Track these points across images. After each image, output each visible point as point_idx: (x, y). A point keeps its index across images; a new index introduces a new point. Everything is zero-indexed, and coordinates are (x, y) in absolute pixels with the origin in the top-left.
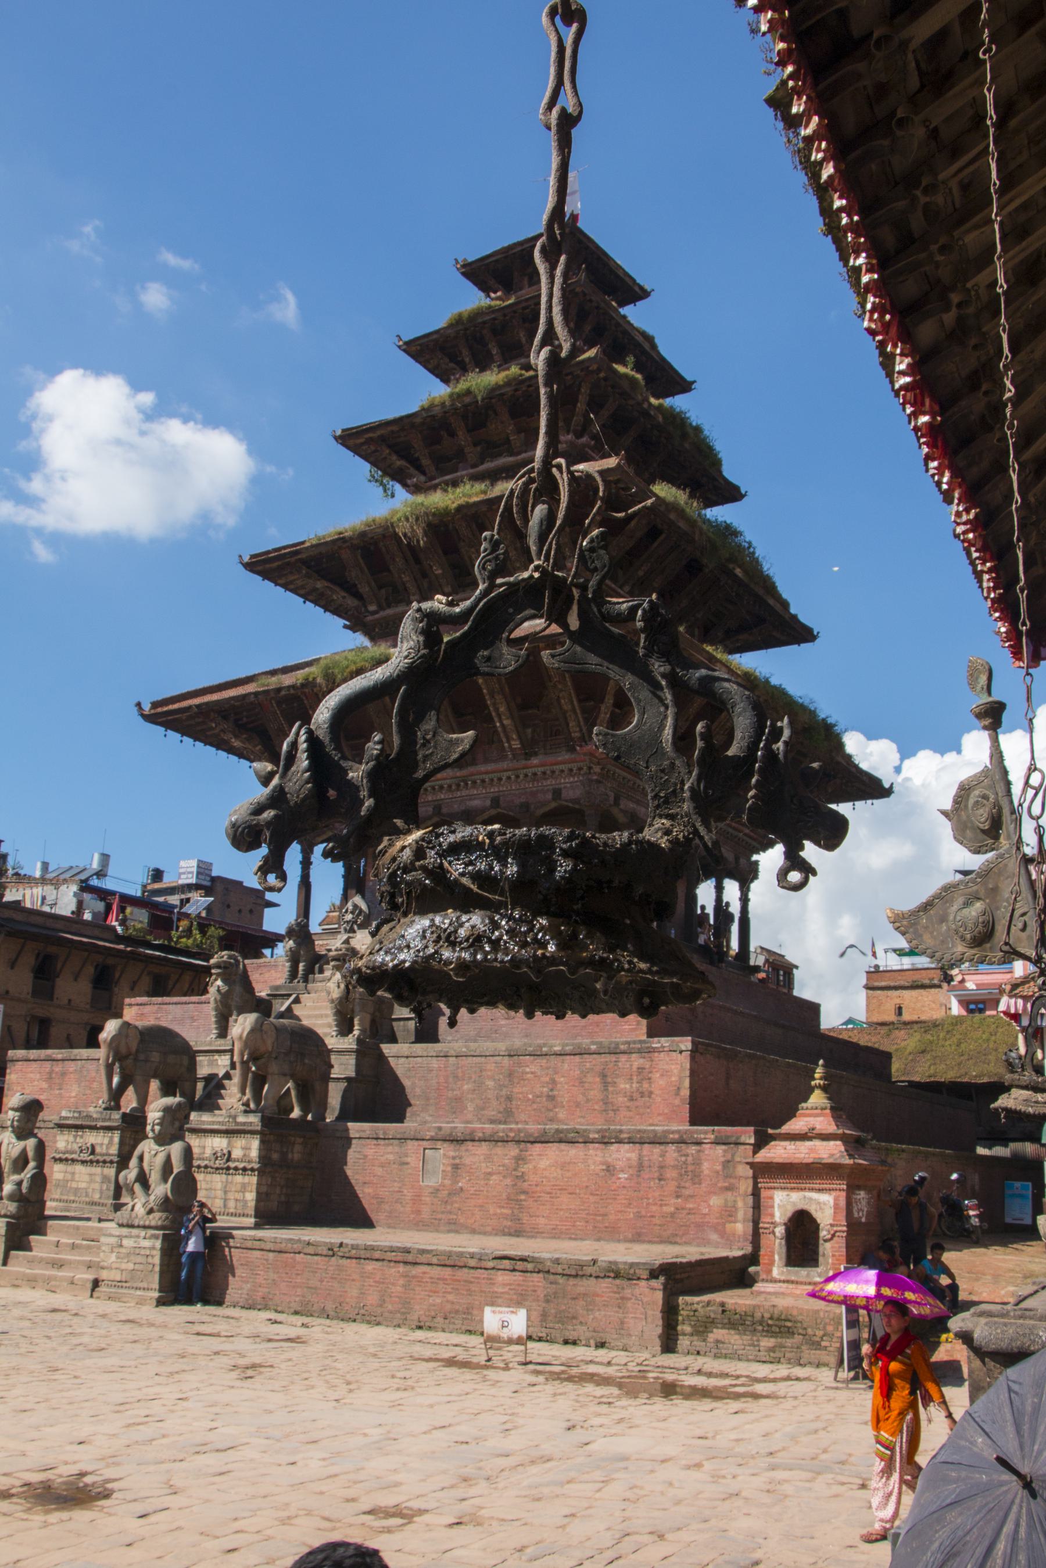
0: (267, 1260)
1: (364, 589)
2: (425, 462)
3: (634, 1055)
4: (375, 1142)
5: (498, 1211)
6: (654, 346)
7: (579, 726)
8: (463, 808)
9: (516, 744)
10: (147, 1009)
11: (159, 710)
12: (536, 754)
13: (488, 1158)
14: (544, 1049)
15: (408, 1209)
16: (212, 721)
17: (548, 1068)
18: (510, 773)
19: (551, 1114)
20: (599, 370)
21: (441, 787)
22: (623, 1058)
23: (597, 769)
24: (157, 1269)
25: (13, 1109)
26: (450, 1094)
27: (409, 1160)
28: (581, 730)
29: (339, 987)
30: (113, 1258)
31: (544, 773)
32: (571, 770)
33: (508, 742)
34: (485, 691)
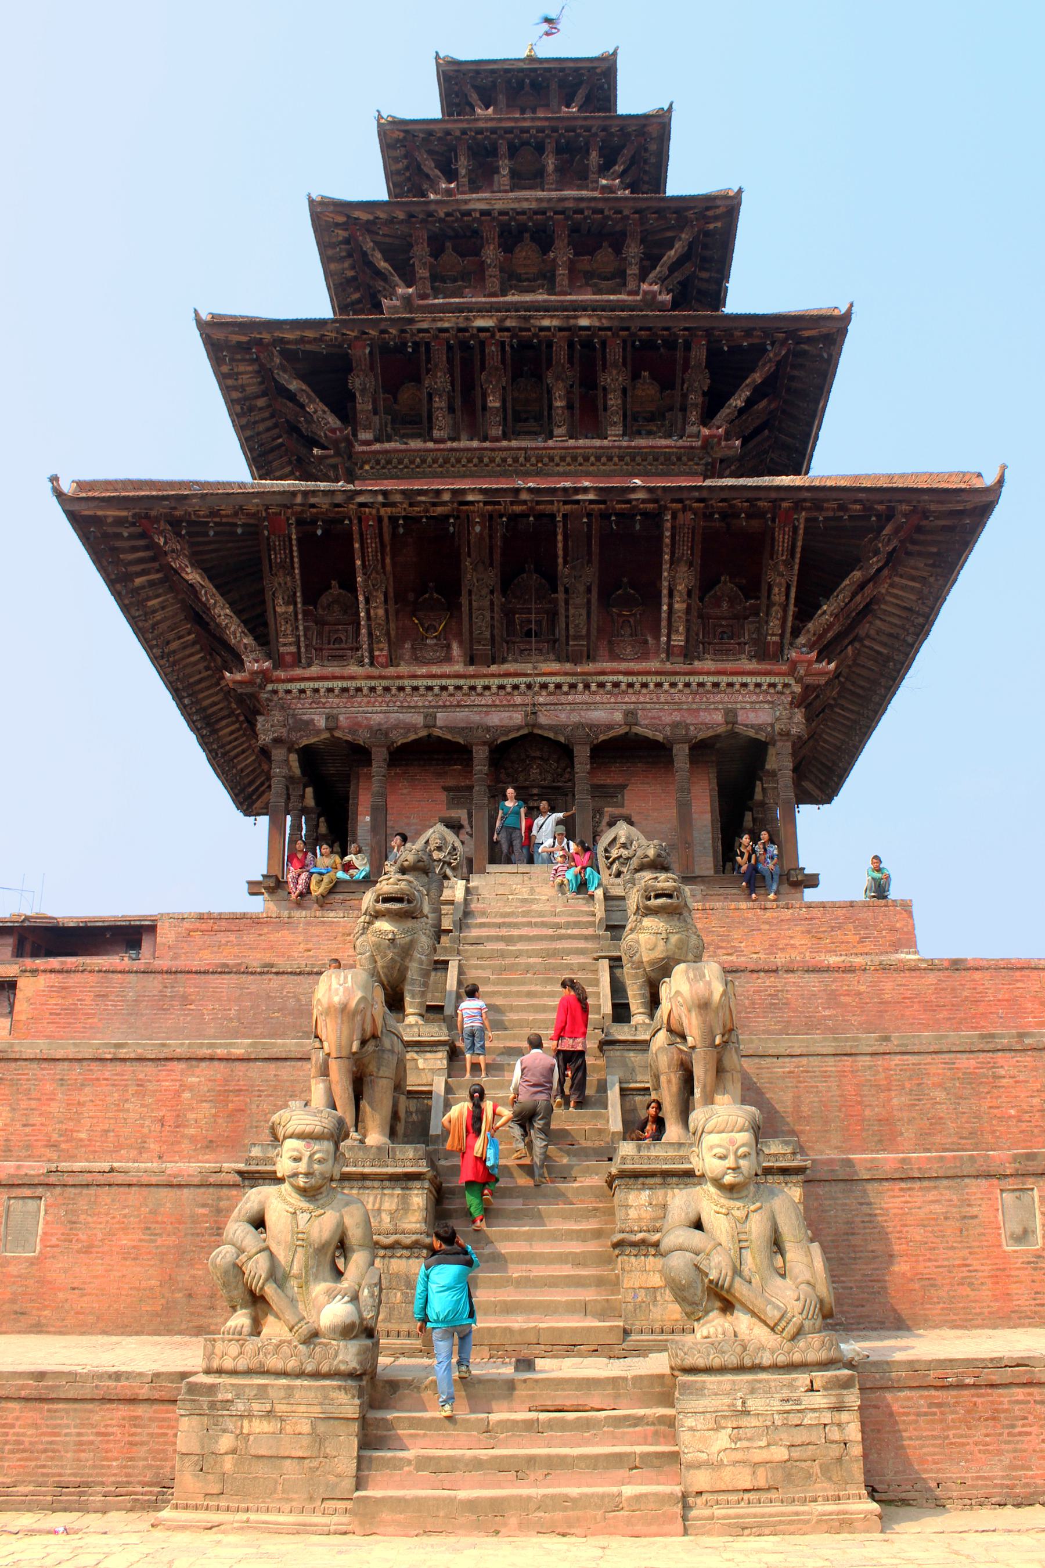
1: (363, 405)
2: (423, 272)
4: (903, 1185)
7: (783, 626)
8: (575, 718)
9: (679, 640)
10: (74, 980)
15: (986, 1293)
16: (161, 533)
18: (663, 678)
20: (716, 218)
21: (544, 686)
24: (857, 1450)
25: (300, 1136)
27: (975, 1211)
28: (782, 636)
29: (667, 940)
30: (722, 1440)
31: (716, 685)
32: (758, 685)
33: (669, 636)
34: (667, 557)
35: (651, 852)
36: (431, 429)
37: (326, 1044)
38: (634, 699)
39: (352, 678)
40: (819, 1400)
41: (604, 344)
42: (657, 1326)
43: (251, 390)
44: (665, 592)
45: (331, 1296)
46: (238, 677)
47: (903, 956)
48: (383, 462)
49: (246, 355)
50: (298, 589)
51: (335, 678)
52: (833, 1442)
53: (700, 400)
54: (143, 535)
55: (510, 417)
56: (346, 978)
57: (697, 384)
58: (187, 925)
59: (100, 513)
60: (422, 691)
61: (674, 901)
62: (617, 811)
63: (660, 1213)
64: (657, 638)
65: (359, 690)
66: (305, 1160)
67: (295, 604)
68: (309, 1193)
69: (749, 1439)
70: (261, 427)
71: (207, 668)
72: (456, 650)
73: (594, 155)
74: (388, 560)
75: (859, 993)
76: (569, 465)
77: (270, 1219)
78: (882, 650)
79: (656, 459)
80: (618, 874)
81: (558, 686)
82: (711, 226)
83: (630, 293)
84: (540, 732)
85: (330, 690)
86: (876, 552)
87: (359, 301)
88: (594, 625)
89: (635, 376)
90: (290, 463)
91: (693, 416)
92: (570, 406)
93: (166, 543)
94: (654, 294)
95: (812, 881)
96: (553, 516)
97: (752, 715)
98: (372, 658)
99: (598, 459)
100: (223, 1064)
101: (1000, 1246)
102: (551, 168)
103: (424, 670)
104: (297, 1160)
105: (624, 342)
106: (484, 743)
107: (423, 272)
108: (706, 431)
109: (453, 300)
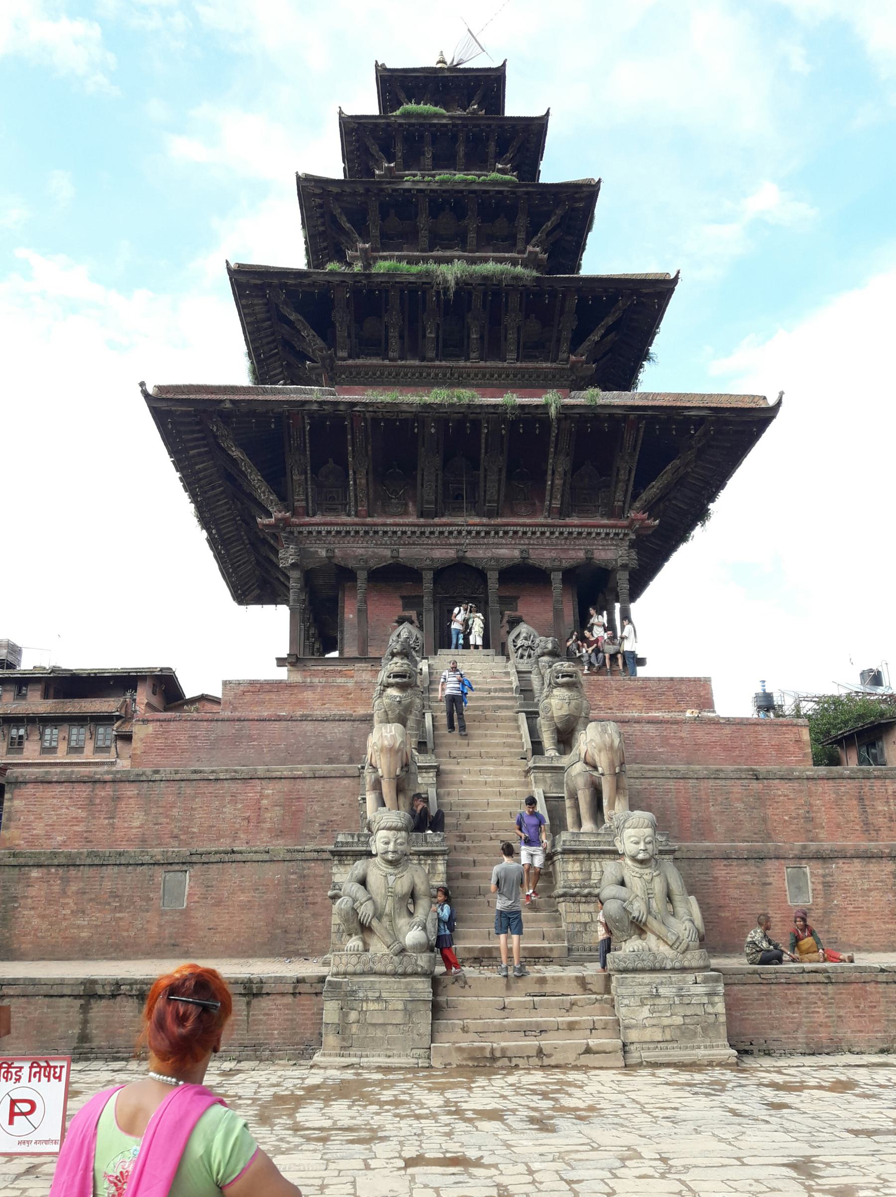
0: (826, 994)
1: (341, 333)
3: (887, 781)
4: (725, 862)
5: (883, 927)
7: (625, 496)
8: (490, 555)
9: (556, 504)
13: (862, 874)
14: (796, 774)
17: (801, 791)
19: (811, 835)
20: (580, 200)
21: (469, 532)
22: (878, 783)
23: (633, 537)
24: (723, 1019)
25: (389, 829)
26: (694, 816)
27: (770, 880)
28: (624, 502)
30: (645, 1012)
31: (580, 534)
32: (607, 534)
33: (550, 501)
35: (550, 646)
36: (387, 350)
37: (380, 770)
38: (527, 542)
39: (344, 524)
40: (701, 989)
41: (507, 294)
42: (587, 946)
43: (259, 316)
44: (550, 472)
45: (411, 927)
46: (266, 521)
47: (706, 714)
48: (354, 373)
49: (254, 288)
50: (309, 464)
51: (332, 524)
52: (709, 1014)
53: (570, 336)
54: (198, 423)
55: (441, 345)
56: (391, 728)
57: (569, 323)
58: (242, 688)
59: (173, 408)
60: (390, 534)
61: (573, 679)
62: (513, 614)
63: (587, 876)
64: (542, 501)
65: (348, 532)
66: (392, 844)
67: (306, 473)
68: (393, 863)
69: (660, 1012)
70: (265, 341)
71: (228, 509)
72: (411, 508)
74: (370, 448)
75: (681, 738)
76: (480, 379)
77: (371, 880)
78: (682, 506)
79: (538, 377)
80: (522, 657)
81: (478, 533)
82: (577, 205)
83: (519, 253)
84: (466, 562)
85: (329, 532)
86: (690, 448)
87: (325, 248)
88: (502, 493)
89: (527, 317)
90: (282, 366)
91: (565, 347)
92: (482, 338)
93: (217, 430)
94: (536, 253)
95: (641, 662)
96: (480, 421)
97: (603, 553)
99: (500, 376)
100: (287, 781)
101: (786, 902)
103: (390, 521)
104: (387, 843)
105: (521, 294)
106: (430, 569)
107: (375, 232)
108: (573, 358)
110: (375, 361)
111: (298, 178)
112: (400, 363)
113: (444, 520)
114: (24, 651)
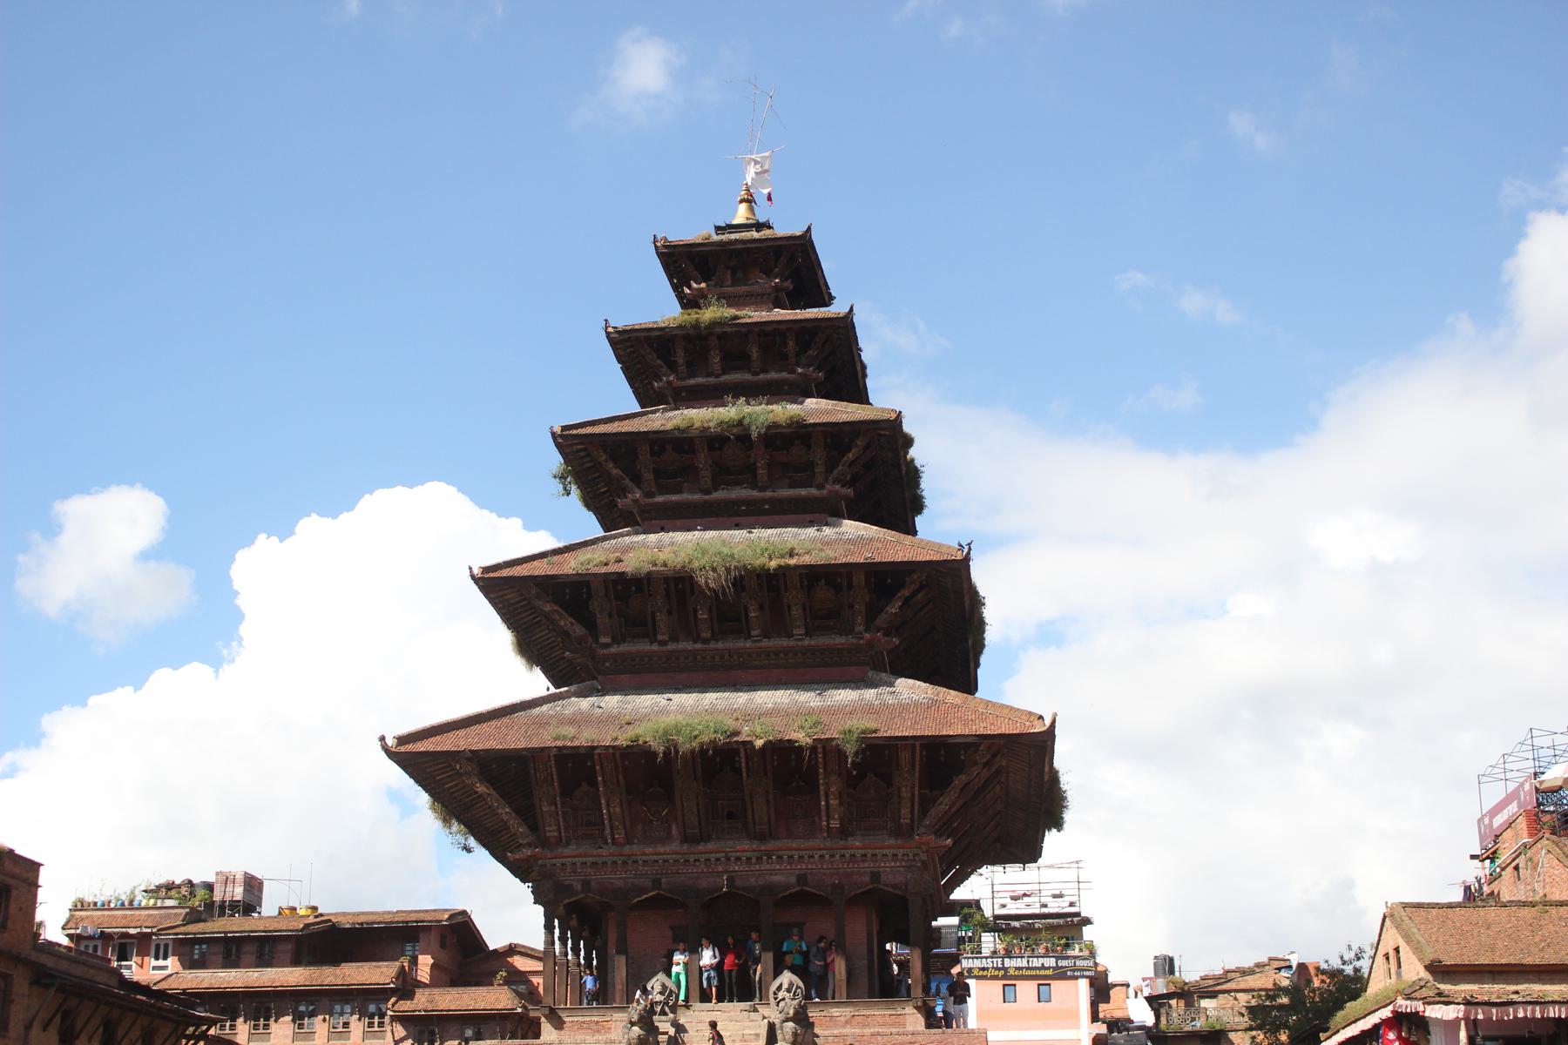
6: (865, 376)
7: (912, 812)
8: (761, 882)
9: (835, 824)
11: (410, 748)
12: (851, 834)
21: (739, 859)
28: (912, 820)
35: (791, 1012)
51: (585, 856)
72: (674, 831)
73: (791, 344)
81: (749, 859)
86: (976, 764)
98: (613, 839)
102: (755, 355)
107: (648, 476)
109: (674, 498)
110: (642, 646)
111: (553, 434)
112: (671, 646)
113: (710, 846)
114: (266, 885)
